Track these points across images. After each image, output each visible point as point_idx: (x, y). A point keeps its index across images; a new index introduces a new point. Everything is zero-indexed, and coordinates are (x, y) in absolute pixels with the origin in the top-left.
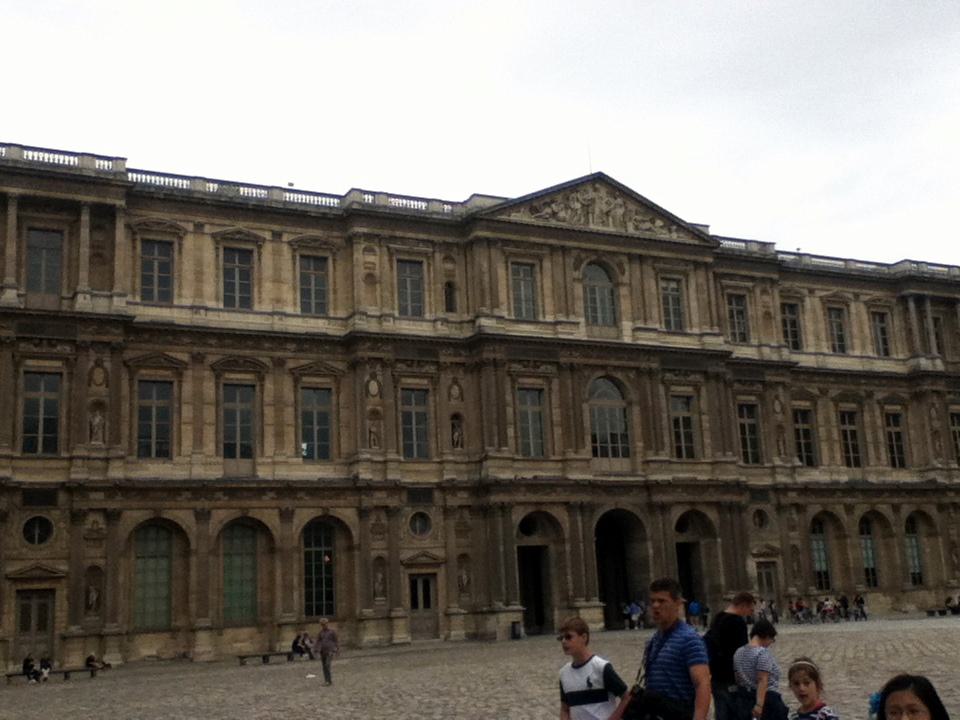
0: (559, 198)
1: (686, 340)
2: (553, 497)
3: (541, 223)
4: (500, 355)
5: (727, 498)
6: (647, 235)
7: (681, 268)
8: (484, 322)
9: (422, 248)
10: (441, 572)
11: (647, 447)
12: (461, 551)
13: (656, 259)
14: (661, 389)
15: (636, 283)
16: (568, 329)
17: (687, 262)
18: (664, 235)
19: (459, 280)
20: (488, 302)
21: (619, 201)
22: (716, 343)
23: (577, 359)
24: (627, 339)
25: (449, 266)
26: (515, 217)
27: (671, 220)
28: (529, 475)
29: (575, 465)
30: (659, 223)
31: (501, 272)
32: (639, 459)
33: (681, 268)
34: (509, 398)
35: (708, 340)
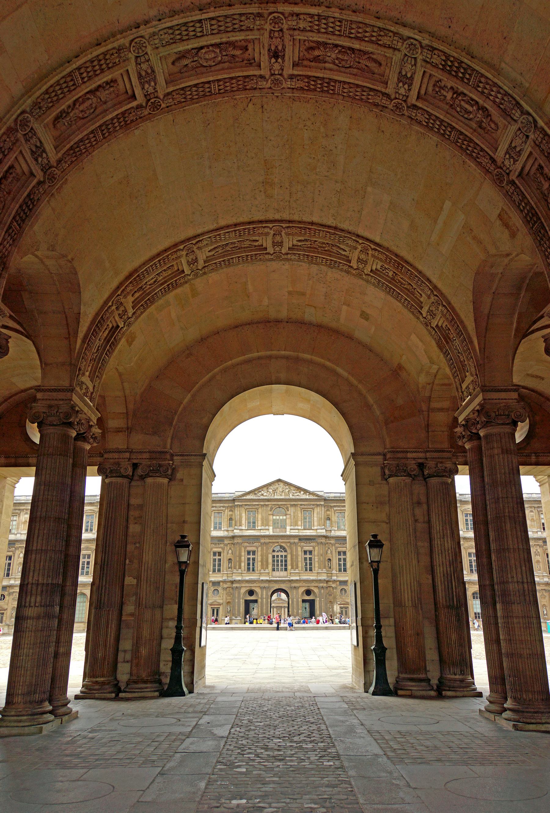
0: (265, 489)
1: (311, 531)
2: (255, 585)
3: (257, 498)
4: (240, 540)
5: (321, 585)
6: (298, 497)
7: (312, 507)
8: (235, 531)
9: (222, 508)
10: (221, 607)
11: (292, 568)
12: (228, 601)
13: (301, 505)
14: (299, 549)
15: (292, 514)
16: (265, 531)
17: (313, 505)
18: (304, 497)
19: (233, 517)
20: (238, 524)
21: (287, 487)
22: (323, 532)
23: (267, 541)
24: (288, 533)
25: (231, 513)
26: (248, 497)
27: (306, 491)
28: (247, 578)
29: (263, 574)
30: (302, 493)
31: (244, 515)
32: (289, 571)
33: (312, 507)
34: (243, 554)
35: (318, 531)
